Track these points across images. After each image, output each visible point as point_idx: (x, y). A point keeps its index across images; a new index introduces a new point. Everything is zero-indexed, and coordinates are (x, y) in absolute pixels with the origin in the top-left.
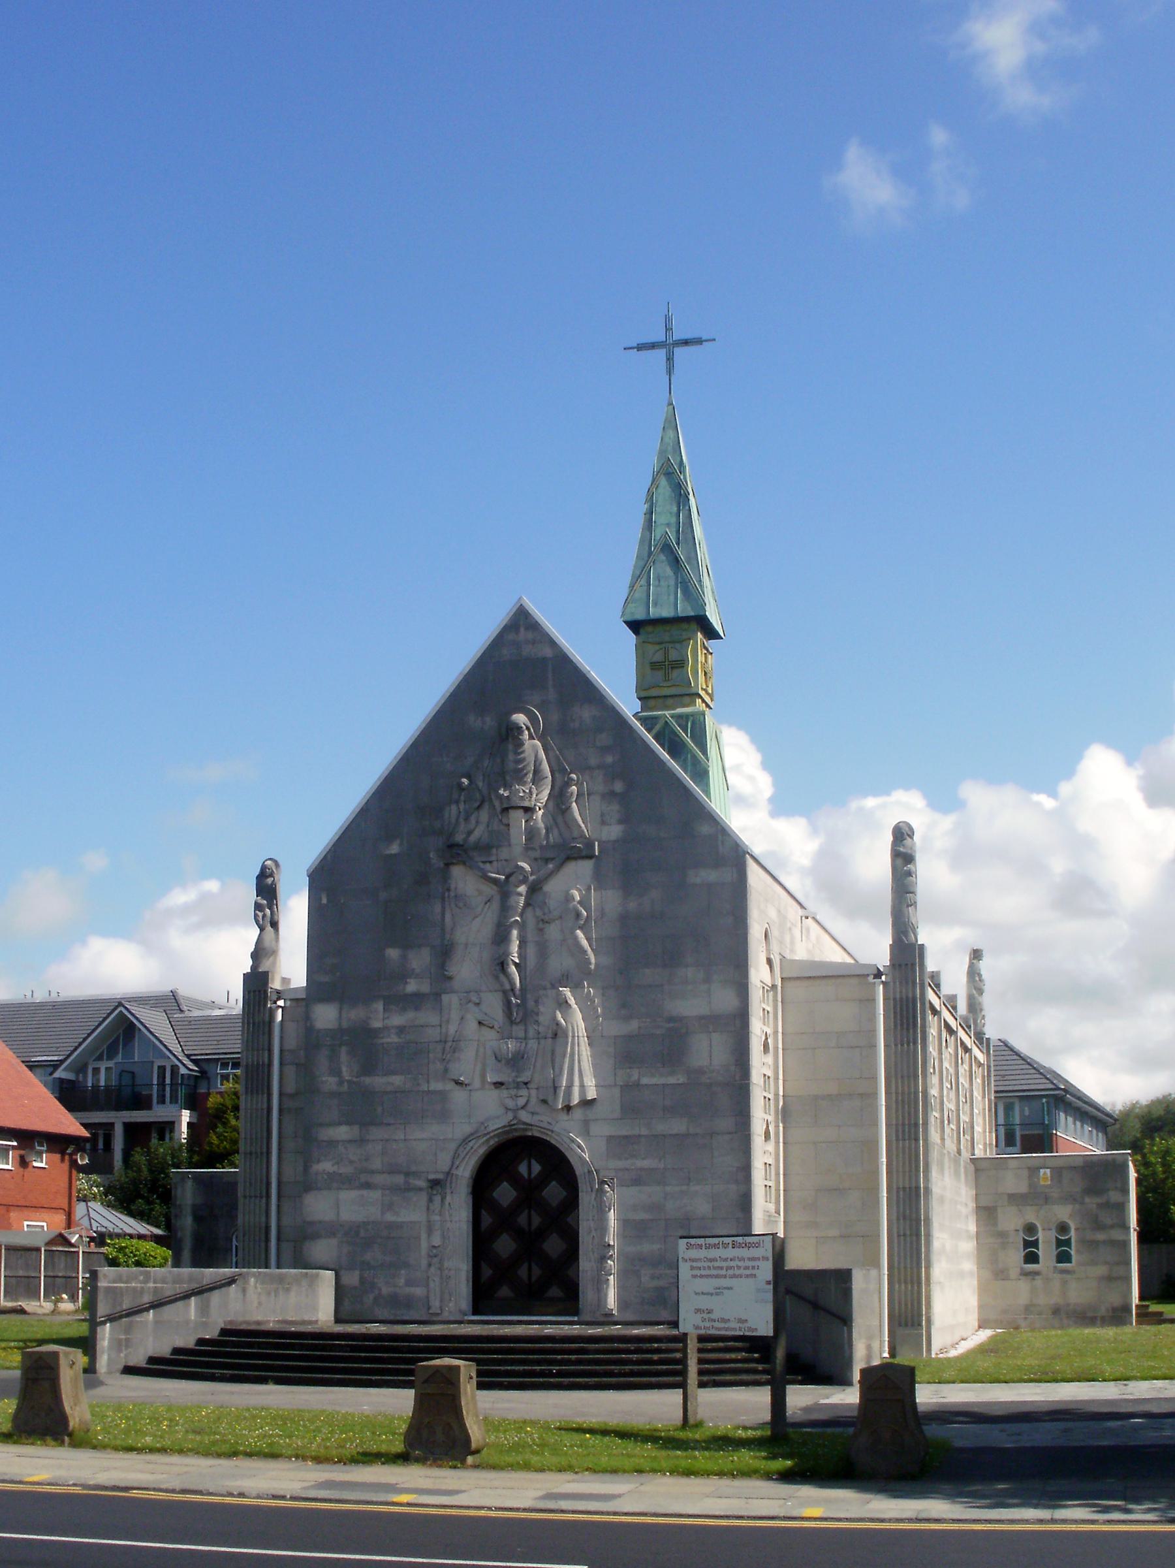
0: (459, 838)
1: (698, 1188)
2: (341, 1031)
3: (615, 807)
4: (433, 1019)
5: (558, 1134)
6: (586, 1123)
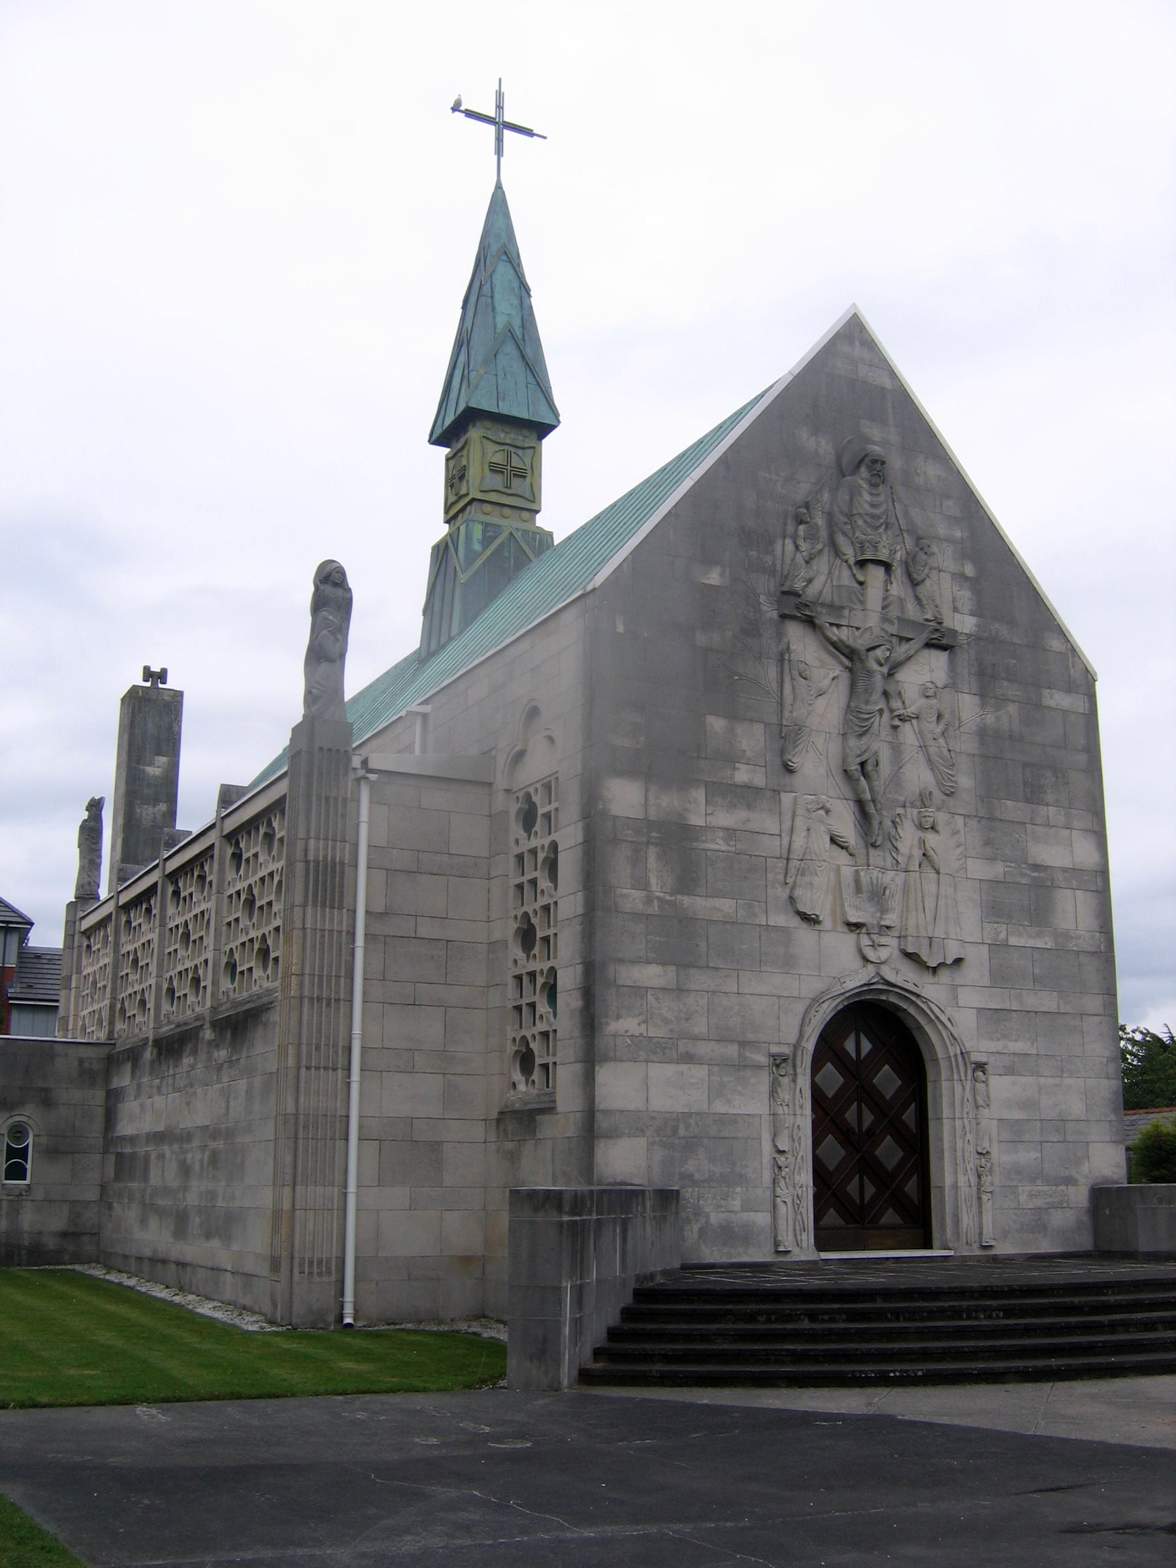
0: (799, 585)
1: (1071, 1081)
2: (650, 824)
3: (967, 594)
4: (771, 825)
5: (926, 1001)
6: (954, 988)
